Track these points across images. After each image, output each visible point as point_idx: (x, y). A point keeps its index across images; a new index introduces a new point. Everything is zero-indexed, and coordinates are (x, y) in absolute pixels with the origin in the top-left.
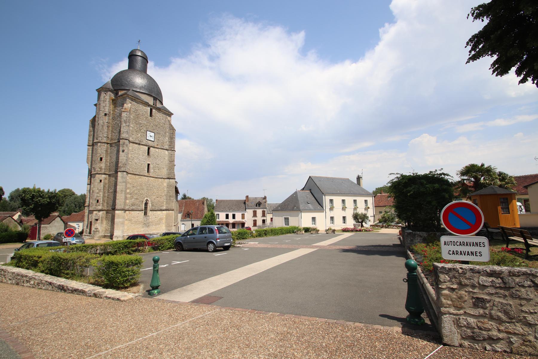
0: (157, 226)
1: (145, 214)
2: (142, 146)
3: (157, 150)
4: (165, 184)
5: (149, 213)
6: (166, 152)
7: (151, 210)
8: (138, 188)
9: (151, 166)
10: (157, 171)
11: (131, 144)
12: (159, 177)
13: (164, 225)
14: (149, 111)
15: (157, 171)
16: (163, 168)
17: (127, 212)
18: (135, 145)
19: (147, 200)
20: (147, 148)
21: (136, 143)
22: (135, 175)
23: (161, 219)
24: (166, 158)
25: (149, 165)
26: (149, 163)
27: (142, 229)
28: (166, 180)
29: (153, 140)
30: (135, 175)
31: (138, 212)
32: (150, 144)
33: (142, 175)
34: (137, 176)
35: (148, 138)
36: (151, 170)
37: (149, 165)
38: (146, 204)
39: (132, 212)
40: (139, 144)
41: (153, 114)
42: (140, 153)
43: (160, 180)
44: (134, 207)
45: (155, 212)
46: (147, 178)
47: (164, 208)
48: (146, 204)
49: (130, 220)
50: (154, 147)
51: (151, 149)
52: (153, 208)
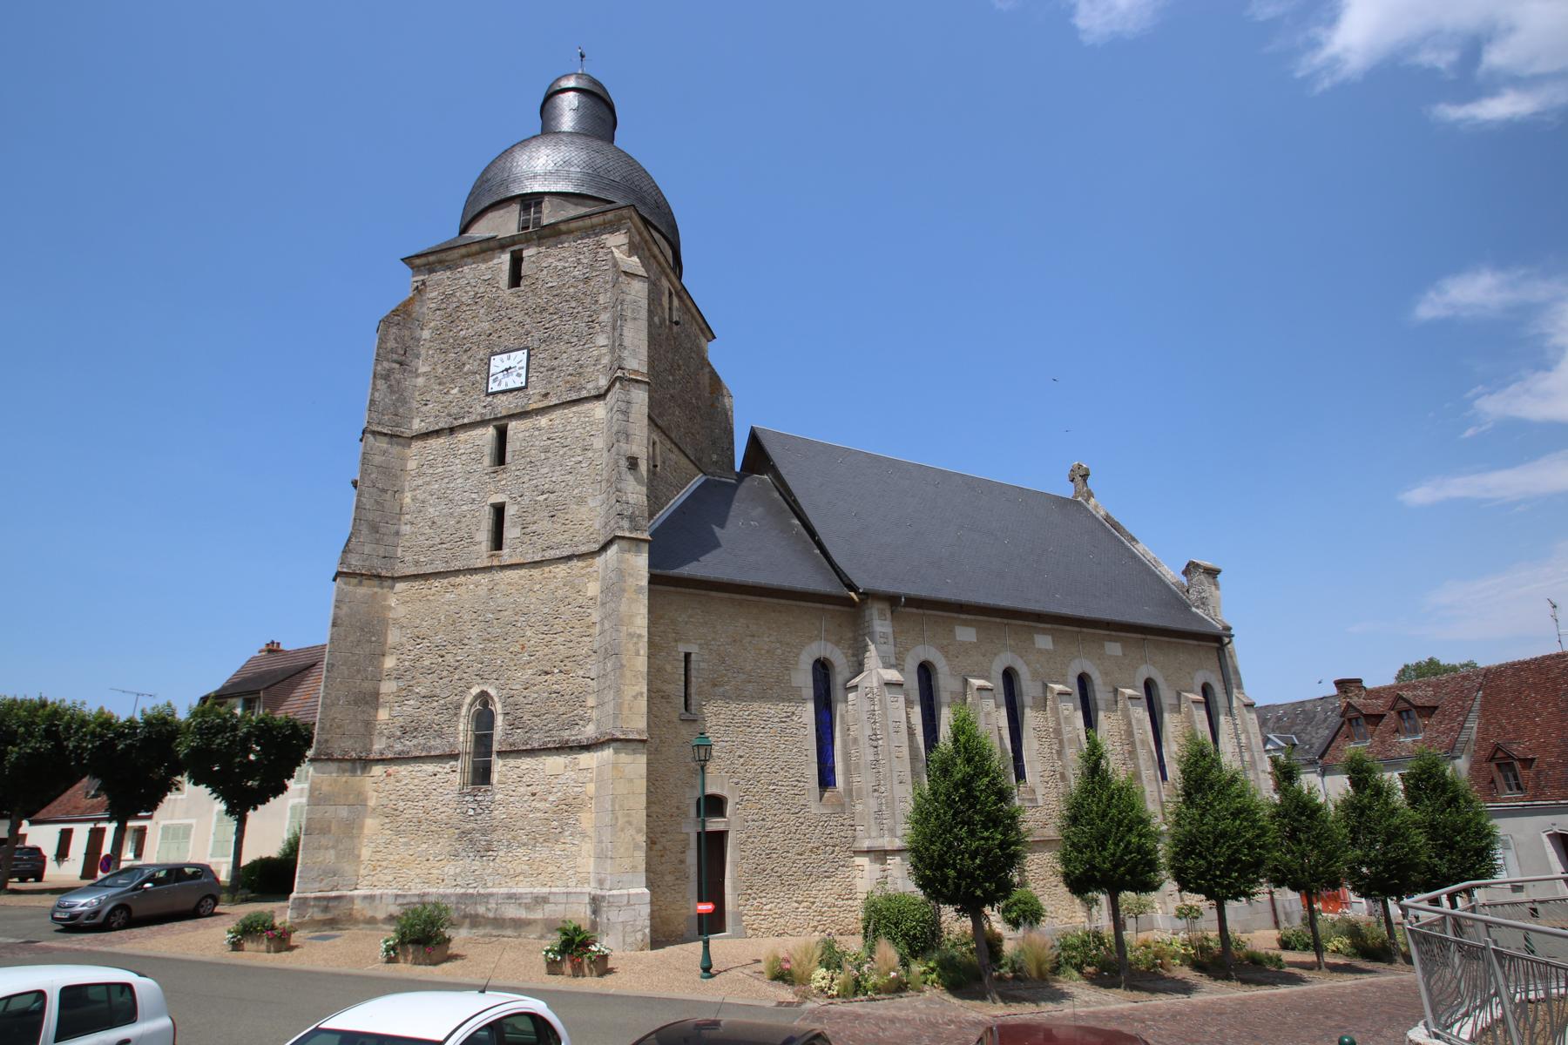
0: (542, 852)
1: (482, 775)
2: (462, 436)
3: (543, 421)
4: (593, 589)
5: (498, 766)
6: (599, 410)
7: (500, 754)
8: (438, 639)
9: (510, 511)
10: (544, 525)
11: (417, 446)
12: (549, 554)
13: (588, 847)
14: (506, 267)
15: (544, 525)
16: (581, 501)
17: (378, 770)
18: (434, 443)
19: (484, 698)
20: (490, 432)
21: (437, 433)
22: (425, 577)
23: (569, 806)
24: (599, 443)
25: (499, 510)
26: (497, 498)
27: (450, 869)
28: (599, 561)
29: (519, 382)
30: (425, 577)
31: (430, 767)
32: (504, 405)
33: (457, 573)
34: (437, 583)
35: (493, 387)
36: (511, 533)
37: (499, 510)
38: (484, 719)
39: (403, 770)
40: (452, 430)
41: (525, 269)
42: (457, 467)
43: (561, 570)
44: (409, 745)
45: (526, 763)
46: (482, 579)
47: (589, 732)
48: (484, 719)
49: (391, 814)
50: (523, 415)
51: (513, 426)
52: (518, 736)
